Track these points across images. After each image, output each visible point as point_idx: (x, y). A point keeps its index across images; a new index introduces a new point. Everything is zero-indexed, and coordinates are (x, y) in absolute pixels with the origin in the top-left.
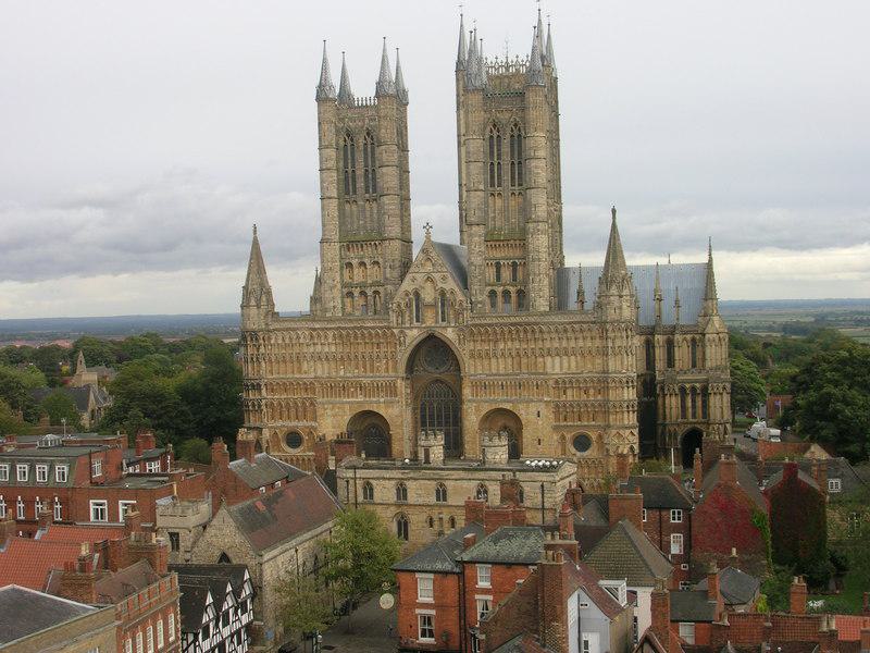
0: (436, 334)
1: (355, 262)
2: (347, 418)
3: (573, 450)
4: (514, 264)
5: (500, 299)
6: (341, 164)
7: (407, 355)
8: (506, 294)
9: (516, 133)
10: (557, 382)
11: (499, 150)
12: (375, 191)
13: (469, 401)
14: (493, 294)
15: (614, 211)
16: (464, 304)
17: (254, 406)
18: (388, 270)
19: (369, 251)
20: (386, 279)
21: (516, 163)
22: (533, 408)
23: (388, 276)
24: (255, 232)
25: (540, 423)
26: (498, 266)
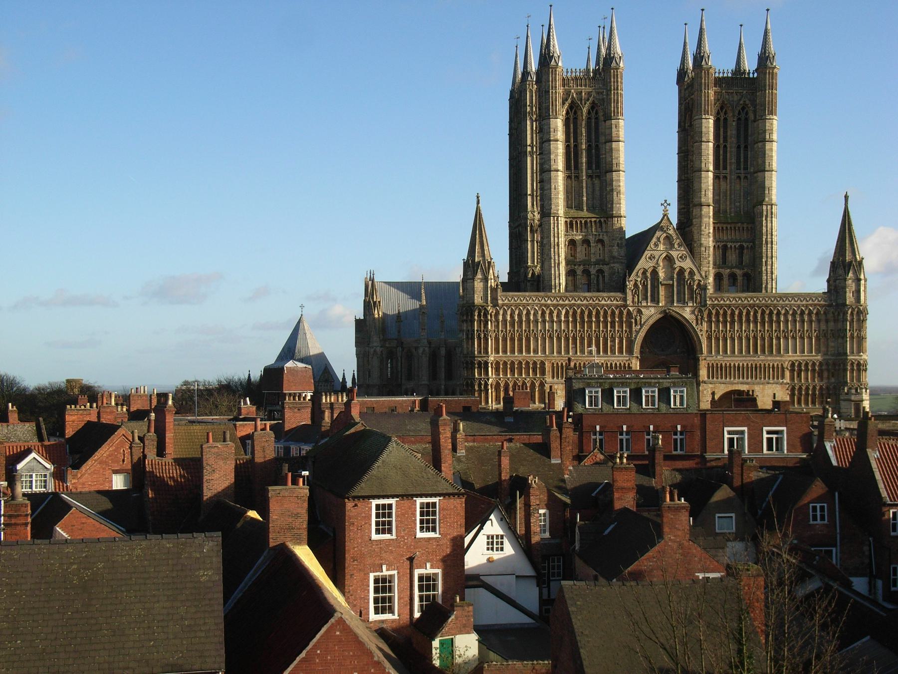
0: (673, 313)
4: (741, 247)
5: (726, 281)
7: (642, 334)
8: (733, 277)
9: (743, 116)
10: (793, 365)
11: (725, 132)
12: (598, 166)
13: (705, 382)
14: (718, 277)
15: (846, 197)
16: (702, 283)
17: (480, 384)
18: (616, 248)
20: (614, 257)
21: (742, 146)
23: (615, 254)
24: (478, 202)
26: (725, 248)
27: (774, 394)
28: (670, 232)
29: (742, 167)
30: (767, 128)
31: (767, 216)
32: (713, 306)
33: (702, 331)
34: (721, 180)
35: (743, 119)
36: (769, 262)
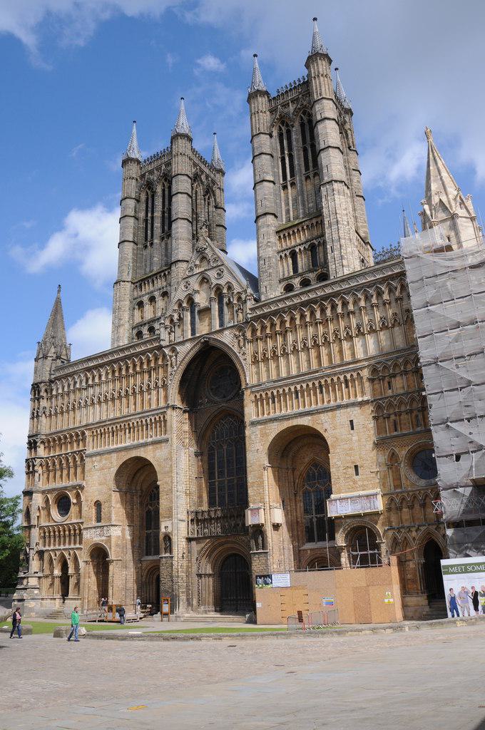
0: (212, 342)
1: (145, 299)
2: (114, 470)
3: (413, 477)
6: (142, 215)
7: (178, 377)
8: (305, 283)
9: (305, 118)
10: (374, 370)
13: (253, 424)
16: (243, 296)
19: (160, 283)
22: (342, 417)
24: (59, 291)
25: (355, 438)
26: (294, 255)
27: (351, 422)
28: (206, 252)
29: (311, 164)
30: (317, 110)
31: (326, 196)
32: (257, 318)
33: (244, 355)
34: (289, 187)
35: (306, 121)
36: (337, 245)
